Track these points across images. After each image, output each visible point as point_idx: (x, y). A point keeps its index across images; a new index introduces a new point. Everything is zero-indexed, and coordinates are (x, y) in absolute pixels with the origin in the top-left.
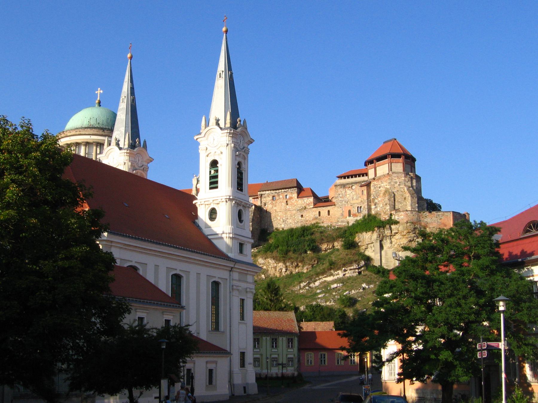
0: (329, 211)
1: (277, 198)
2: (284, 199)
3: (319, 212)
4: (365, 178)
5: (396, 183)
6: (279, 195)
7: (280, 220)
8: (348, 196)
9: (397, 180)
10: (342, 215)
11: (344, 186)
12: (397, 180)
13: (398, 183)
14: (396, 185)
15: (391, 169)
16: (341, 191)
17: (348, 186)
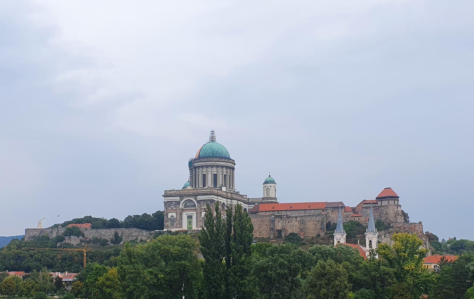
0: (359, 219)
1: (334, 211)
2: (337, 211)
3: (354, 219)
4: (376, 205)
5: (391, 209)
6: (335, 210)
7: (335, 221)
8: (368, 212)
9: (392, 208)
10: (365, 220)
11: (366, 208)
12: (392, 208)
13: (392, 209)
14: (391, 210)
15: (388, 203)
16: (365, 210)
17: (368, 208)
